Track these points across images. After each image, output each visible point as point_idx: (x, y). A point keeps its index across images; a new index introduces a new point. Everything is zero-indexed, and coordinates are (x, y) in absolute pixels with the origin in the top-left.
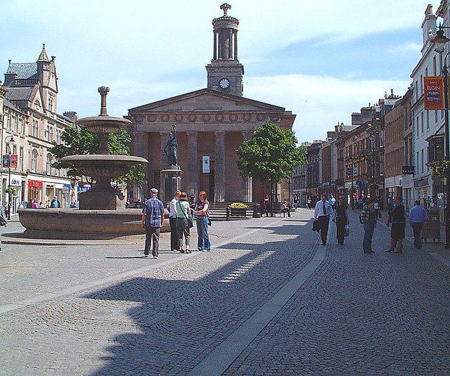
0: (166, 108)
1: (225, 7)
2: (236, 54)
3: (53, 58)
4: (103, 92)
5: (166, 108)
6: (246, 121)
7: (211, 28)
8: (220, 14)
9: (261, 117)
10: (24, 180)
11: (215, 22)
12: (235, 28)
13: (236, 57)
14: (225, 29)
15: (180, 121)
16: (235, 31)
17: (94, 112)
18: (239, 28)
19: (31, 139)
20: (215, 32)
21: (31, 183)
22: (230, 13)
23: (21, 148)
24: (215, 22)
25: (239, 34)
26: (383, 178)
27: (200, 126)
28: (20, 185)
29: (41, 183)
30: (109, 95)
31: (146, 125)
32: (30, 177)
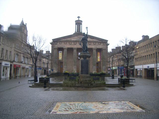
0: (66, 40)
1: (79, 17)
3: (26, 24)
5: (66, 40)
6: (94, 45)
7: (75, 23)
8: (77, 19)
9: (99, 43)
10: (11, 64)
11: (76, 21)
14: (79, 23)
16: (81, 24)
18: (82, 23)
19: (15, 49)
20: (76, 24)
21: (15, 65)
22: (80, 19)
23: (10, 52)
26: (134, 66)
28: (9, 66)
29: (20, 66)
31: (59, 45)
32: (14, 63)
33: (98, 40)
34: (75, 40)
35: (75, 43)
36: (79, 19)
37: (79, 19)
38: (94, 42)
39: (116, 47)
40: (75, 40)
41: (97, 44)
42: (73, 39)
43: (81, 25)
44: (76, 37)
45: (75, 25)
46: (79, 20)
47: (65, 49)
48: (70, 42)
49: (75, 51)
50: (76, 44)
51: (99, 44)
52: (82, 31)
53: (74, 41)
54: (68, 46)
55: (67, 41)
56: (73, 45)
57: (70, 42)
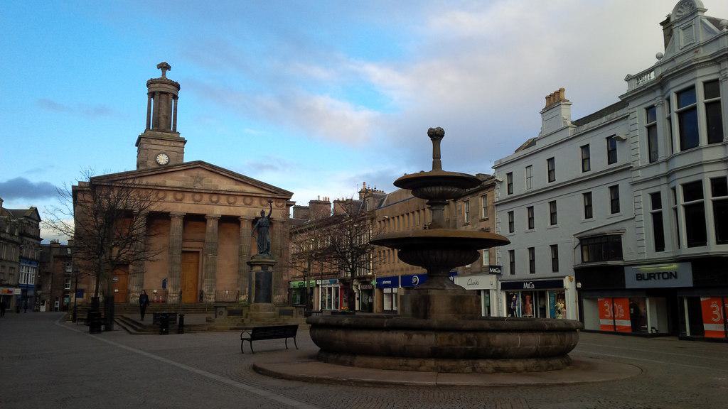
1: (164, 67)
2: (175, 125)
4: (436, 135)
7: (146, 90)
8: (158, 74)
11: (151, 83)
13: (175, 129)
16: (175, 97)
17: (428, 168)
18: (180, 94)
22: (170, 75)
24: (151, 83)
27: (188, 206)
30: (444, 142)
34: (179, 184)
35: (179, 196)
36: (164, 74)
37: (164, 74)
38: (245, 196)
39: (311, 202)
40: (178, 185)
41: (256, 202)
44: (182, 175)
45: (146, 97)
46: (163, 81)
50: (181, 200)
53: (174, 190)
56: (171, 202)
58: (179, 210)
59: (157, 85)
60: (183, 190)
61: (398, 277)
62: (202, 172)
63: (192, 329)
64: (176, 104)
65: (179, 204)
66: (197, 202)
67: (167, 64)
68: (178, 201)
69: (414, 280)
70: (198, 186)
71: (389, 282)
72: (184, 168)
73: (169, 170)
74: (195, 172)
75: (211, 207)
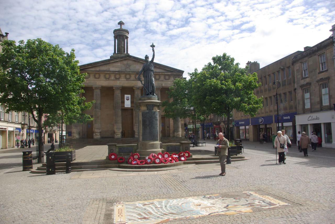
1: (121, 23)
5: (98, 69)
8: (118, 27)
9: (167, 77)
11: (115, 31)
12: (127, 35)
15: (108, 79)
20: (115, 37)
22: (123, 27)
25: (129, 39)
33: (165, 71)
34: (117, 69)
36: (121, 26)
37: (121, 26)
40: (117, 70)
42: (112, 68)
43: (126, 40)
44: (119, 64)
46: (121, 30)
47: (97, 88)
48: (107, 74)
49: (118, 93)
50: (119, 79)
51: (166, 79)
52: (129, 53)
54: (103, 82)
55: (99, 73)
56: (113, 80)
57: (107, 74)
58: (118, 85)
59: (118, 32)
60: (120, 73)
61: (249, 119)
62: (130, 62)
63: (81, 167)
64: (127, 41)
65: (118, 81)
66: (127, 79)
67: (122, 22)
68: (117, 79)
69: (260, 120)
70: (128, 70)
71: (243, 123)
72: (119, 60)
73: (111, 62)
74: (125, 62)
75: (136, 81)
